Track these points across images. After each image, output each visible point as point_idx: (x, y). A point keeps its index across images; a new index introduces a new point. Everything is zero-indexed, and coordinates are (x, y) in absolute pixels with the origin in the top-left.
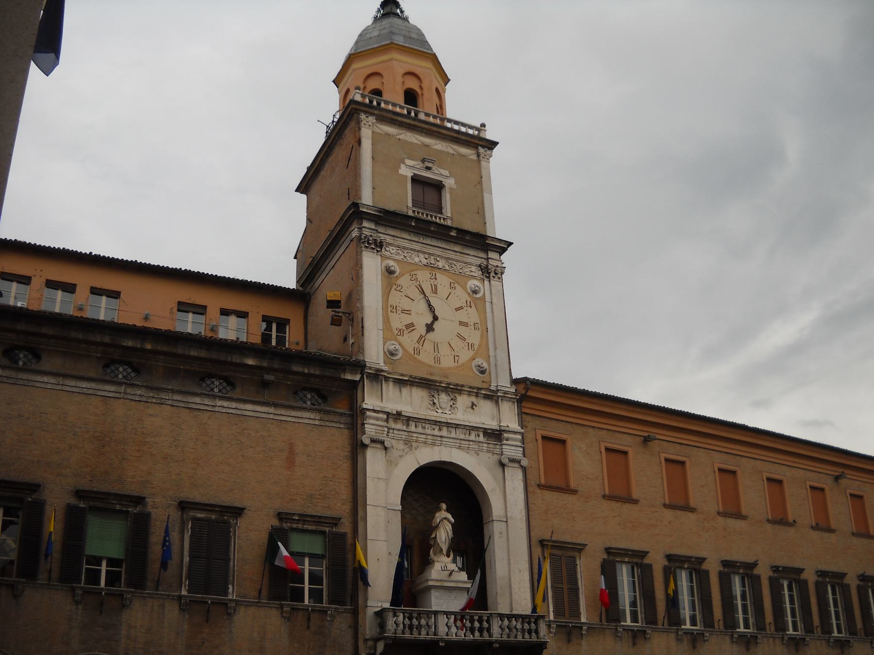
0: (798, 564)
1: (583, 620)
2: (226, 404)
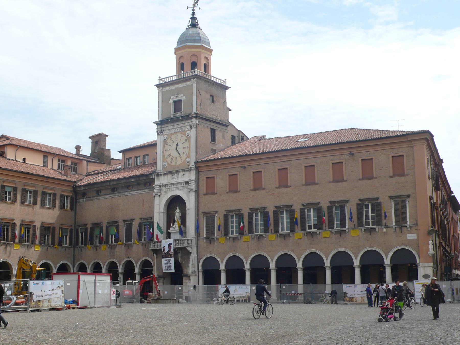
0: (317, 201)
1: (216, 236)
2: (131, 192)
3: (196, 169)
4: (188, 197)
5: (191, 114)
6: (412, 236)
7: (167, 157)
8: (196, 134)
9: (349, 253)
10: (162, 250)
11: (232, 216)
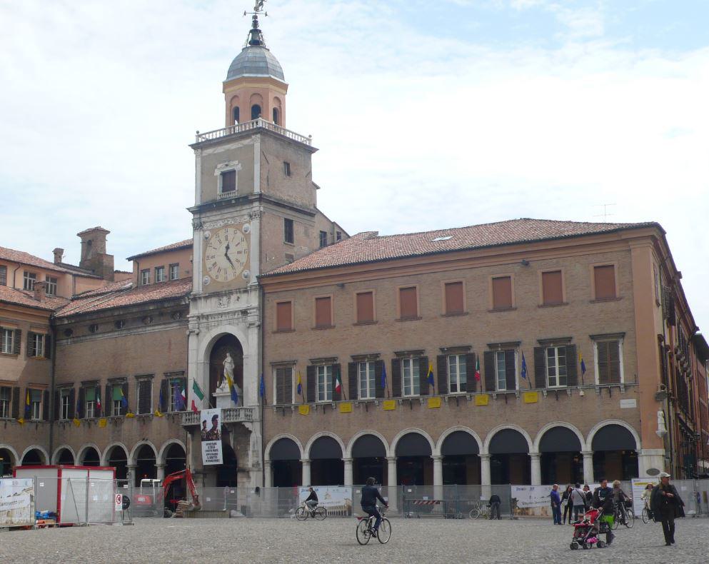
1: (293, 403)
3: (260, 289)
4: (247, 336)
5: (252, 195)
6: (628, 403)
8: (260, 229)
9: (521, 431)
10: (202, 427)
11: (321, 369)
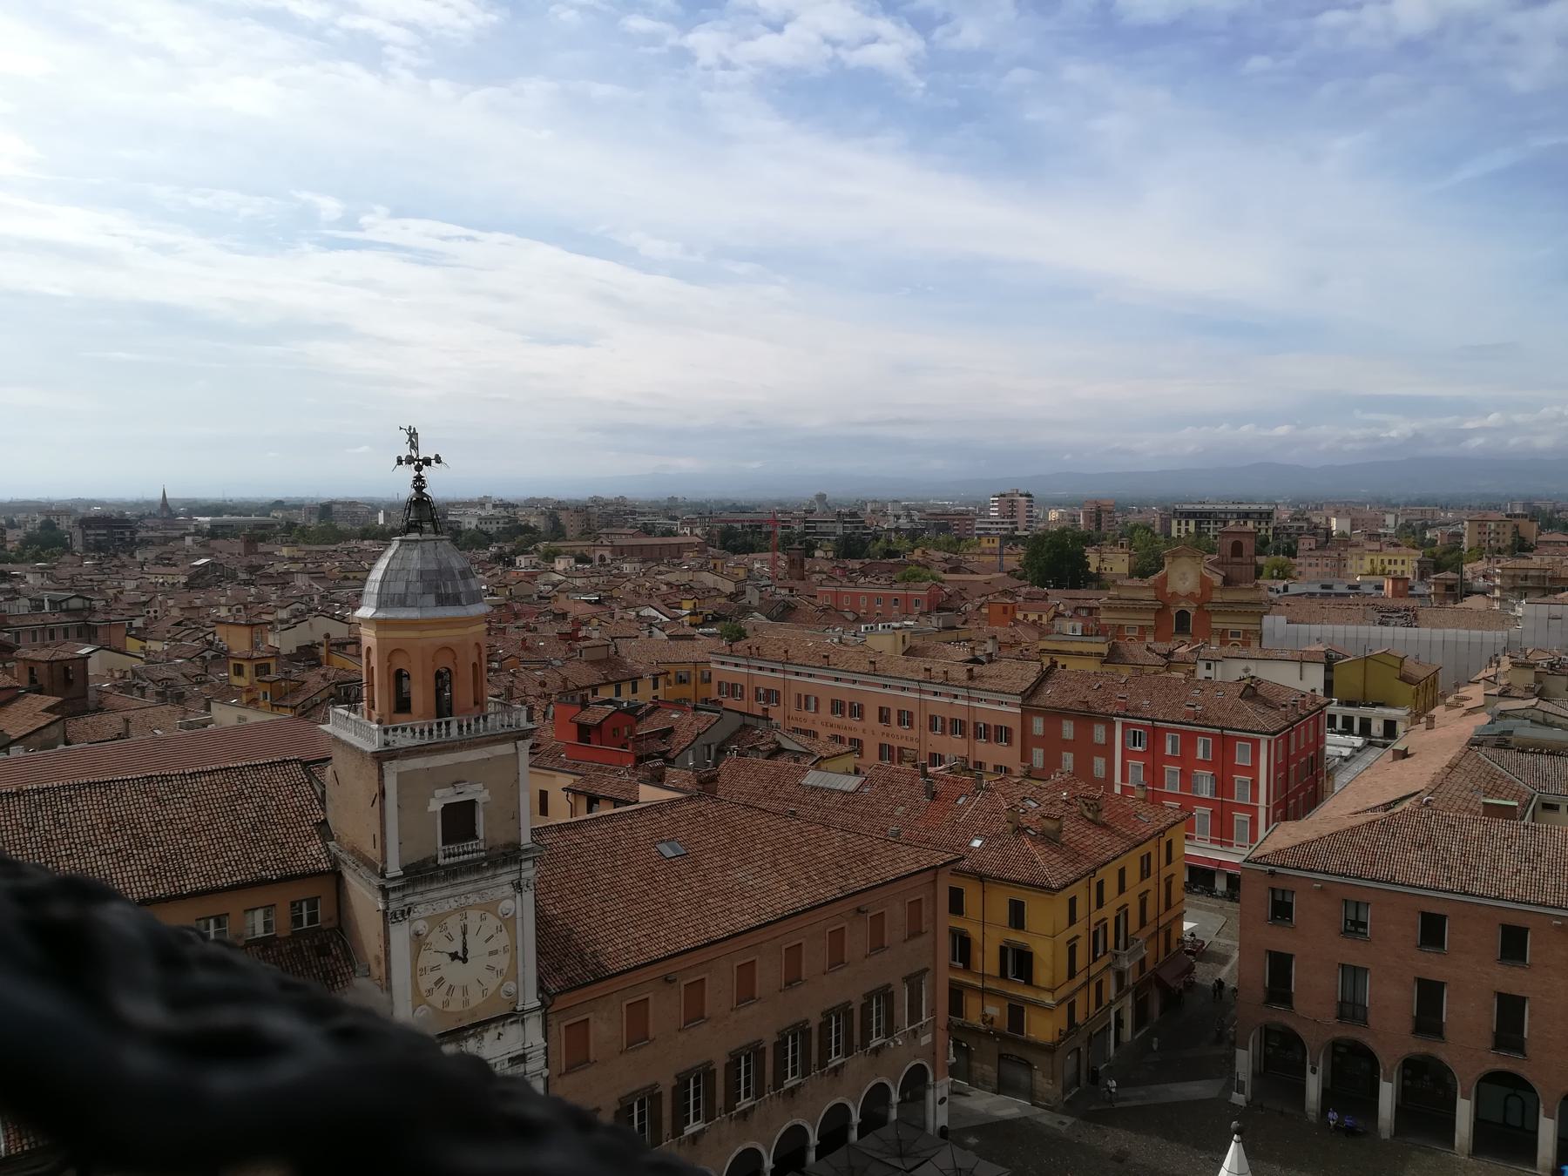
7: (430, 991)
